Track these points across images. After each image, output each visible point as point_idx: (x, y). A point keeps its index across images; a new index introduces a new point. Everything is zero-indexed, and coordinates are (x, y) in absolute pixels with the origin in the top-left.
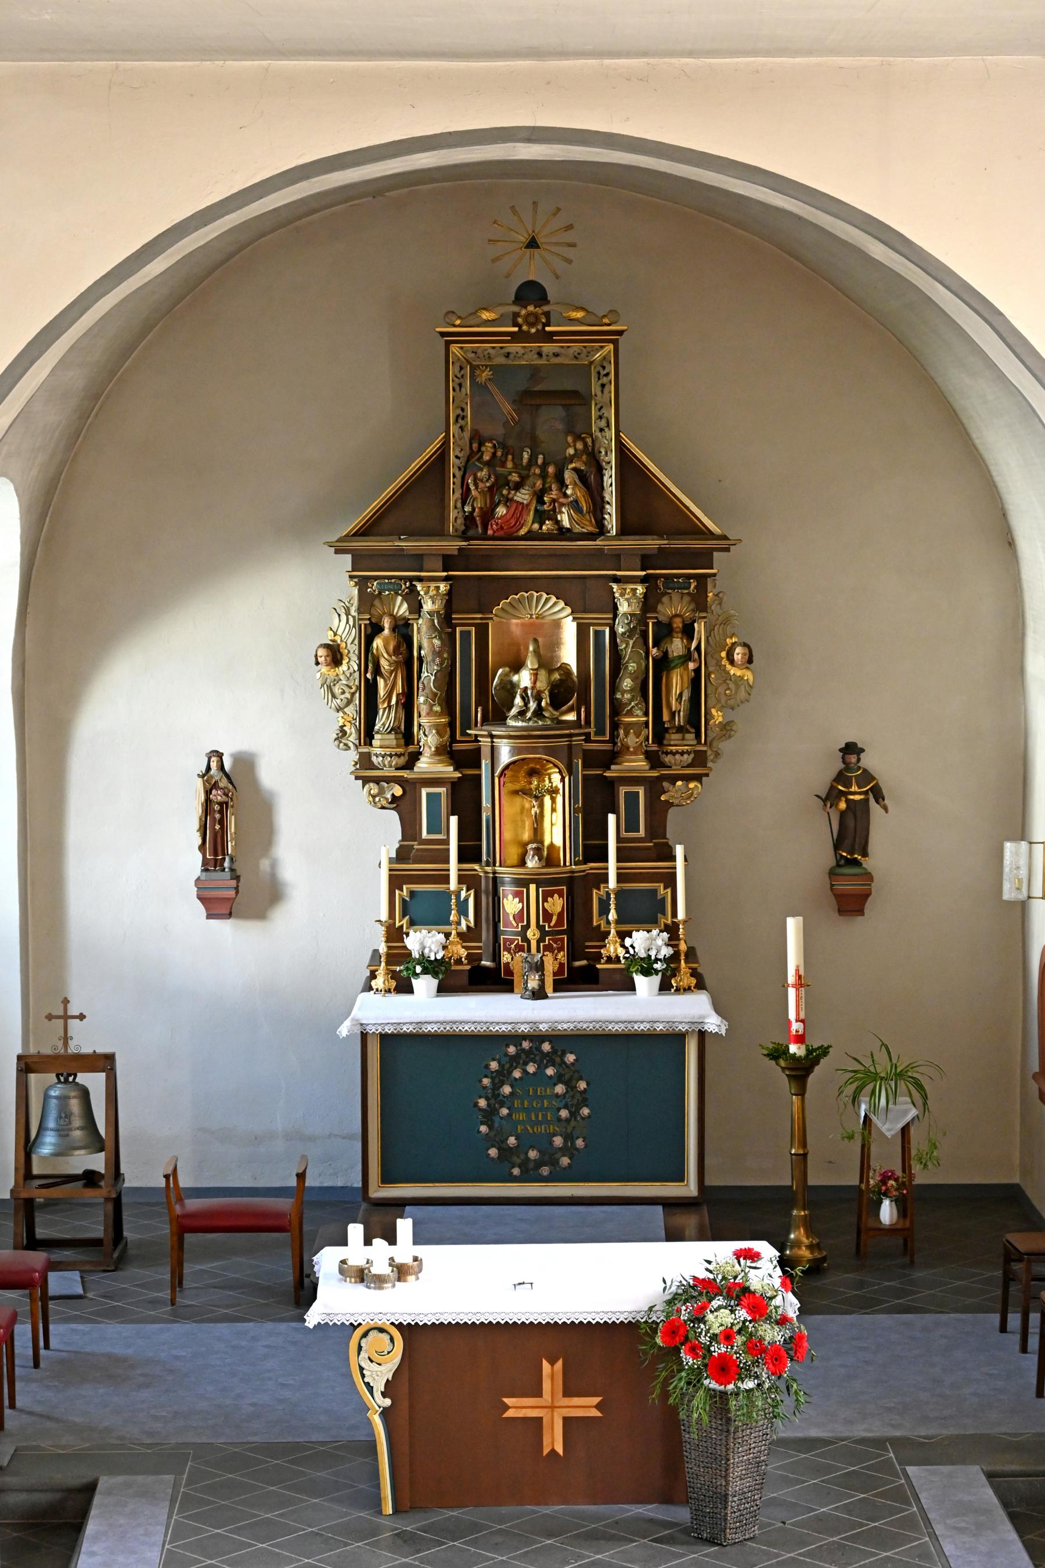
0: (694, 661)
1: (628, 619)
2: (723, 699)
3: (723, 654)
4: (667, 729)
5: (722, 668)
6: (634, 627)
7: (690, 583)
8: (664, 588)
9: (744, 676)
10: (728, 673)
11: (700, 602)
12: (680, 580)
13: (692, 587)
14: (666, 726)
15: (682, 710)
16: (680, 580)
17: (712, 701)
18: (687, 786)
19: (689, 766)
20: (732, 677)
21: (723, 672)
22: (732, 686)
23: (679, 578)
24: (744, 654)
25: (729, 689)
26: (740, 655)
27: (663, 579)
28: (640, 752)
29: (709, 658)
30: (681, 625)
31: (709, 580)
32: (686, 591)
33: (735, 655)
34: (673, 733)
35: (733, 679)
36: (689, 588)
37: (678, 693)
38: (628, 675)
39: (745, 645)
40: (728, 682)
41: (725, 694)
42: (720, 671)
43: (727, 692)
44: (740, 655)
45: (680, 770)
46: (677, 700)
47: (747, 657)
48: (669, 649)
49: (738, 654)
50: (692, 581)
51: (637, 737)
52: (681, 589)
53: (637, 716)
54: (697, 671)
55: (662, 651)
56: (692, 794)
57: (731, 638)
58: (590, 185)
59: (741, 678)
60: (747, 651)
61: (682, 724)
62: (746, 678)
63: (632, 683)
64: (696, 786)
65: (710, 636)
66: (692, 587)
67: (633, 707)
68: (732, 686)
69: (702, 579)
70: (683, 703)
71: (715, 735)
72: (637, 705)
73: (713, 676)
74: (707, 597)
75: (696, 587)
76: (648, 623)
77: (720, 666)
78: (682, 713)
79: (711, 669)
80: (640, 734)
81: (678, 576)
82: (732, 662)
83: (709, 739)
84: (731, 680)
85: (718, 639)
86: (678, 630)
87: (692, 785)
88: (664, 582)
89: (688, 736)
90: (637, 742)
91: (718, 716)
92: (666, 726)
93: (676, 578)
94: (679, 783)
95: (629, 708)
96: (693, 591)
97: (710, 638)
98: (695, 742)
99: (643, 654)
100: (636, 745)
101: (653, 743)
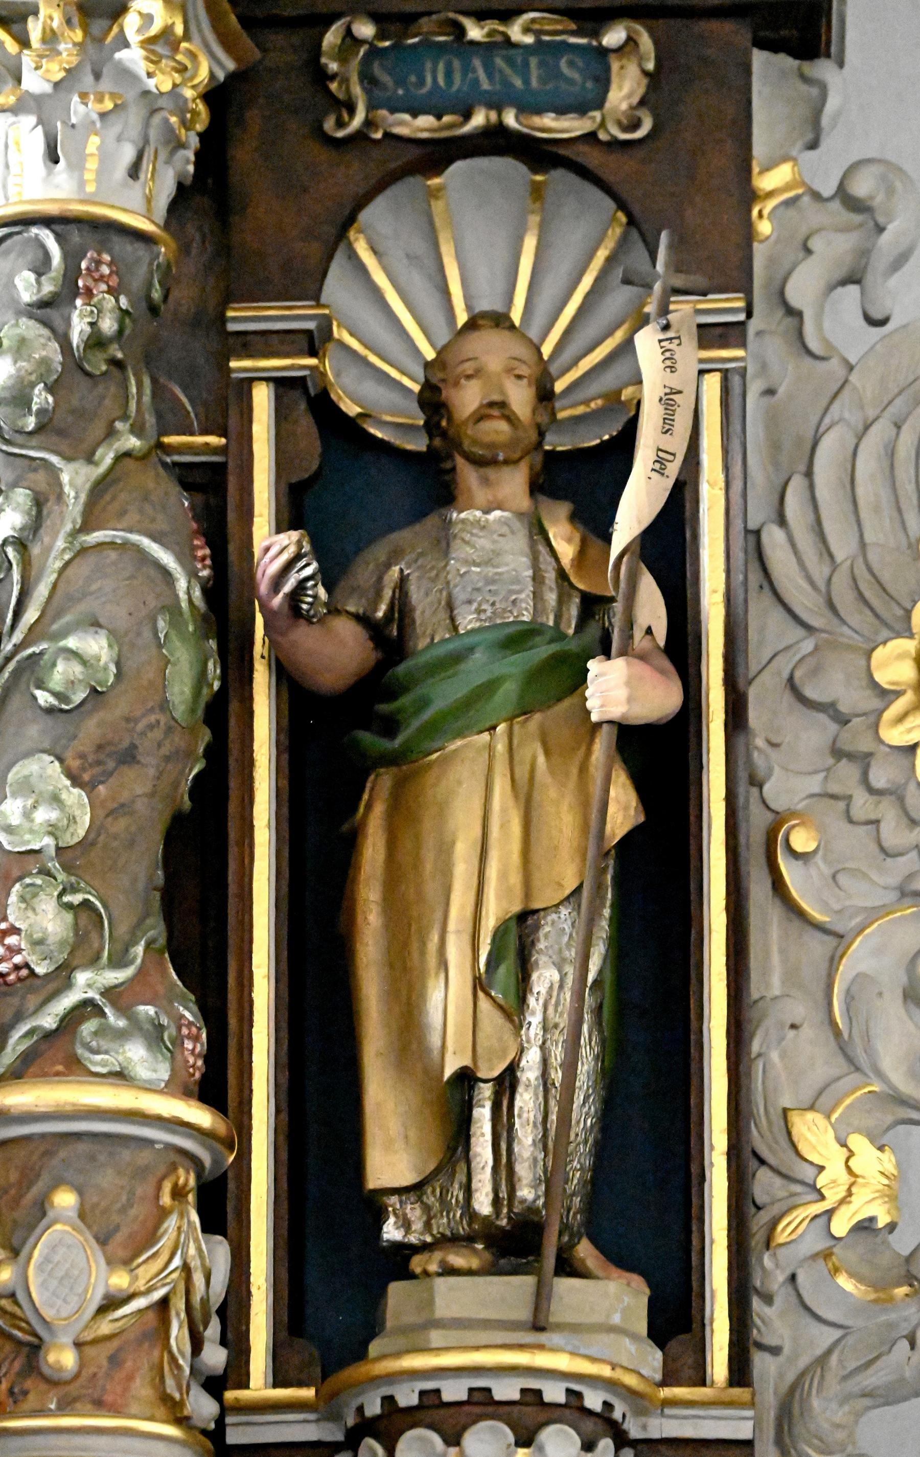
1: (41, 268)
4: (404, 1251)
5: (880, 777)
6: (96, 341)
8: (371, 107)
12: (516, 32)
14: (391, 1232)
15: (530, 1072)
16: (516, 32)
21: (888, 813)
23: (507, 16)
27: (365, 30)
28: (142, 1389)
34: (449, 1271)
36: (599, 104)
37: (490, 923)
38: (34, 731)
42: (862, 805)
46: (480, 985)
48: (416, 594)
50: (614, 37)
51: (127, 1262)
52: (526, 108)
53: (121, 1076)
55: (363, 620)
58: (233, 18)
61: (526, 1193)
63: (75, 797)
65: (782, 521)
67: (87, 1008)
70: (535, 1019)
71: (827, 1336)
72: (109, 992)
73: (802, 840)
74: (750, 196)
76: (246, 385)
77: (864, 760)
80: (152, 1237)
85: (843, 547)
86: (498, 429)
88: (374, 53)
90: (111, 1303)
92: (391, 1232)
93: (480, 16)
95: (48, 1020)
97: (774, 537)
99: (182, 584)
100: (105, 1327)
101: (279, 1380)
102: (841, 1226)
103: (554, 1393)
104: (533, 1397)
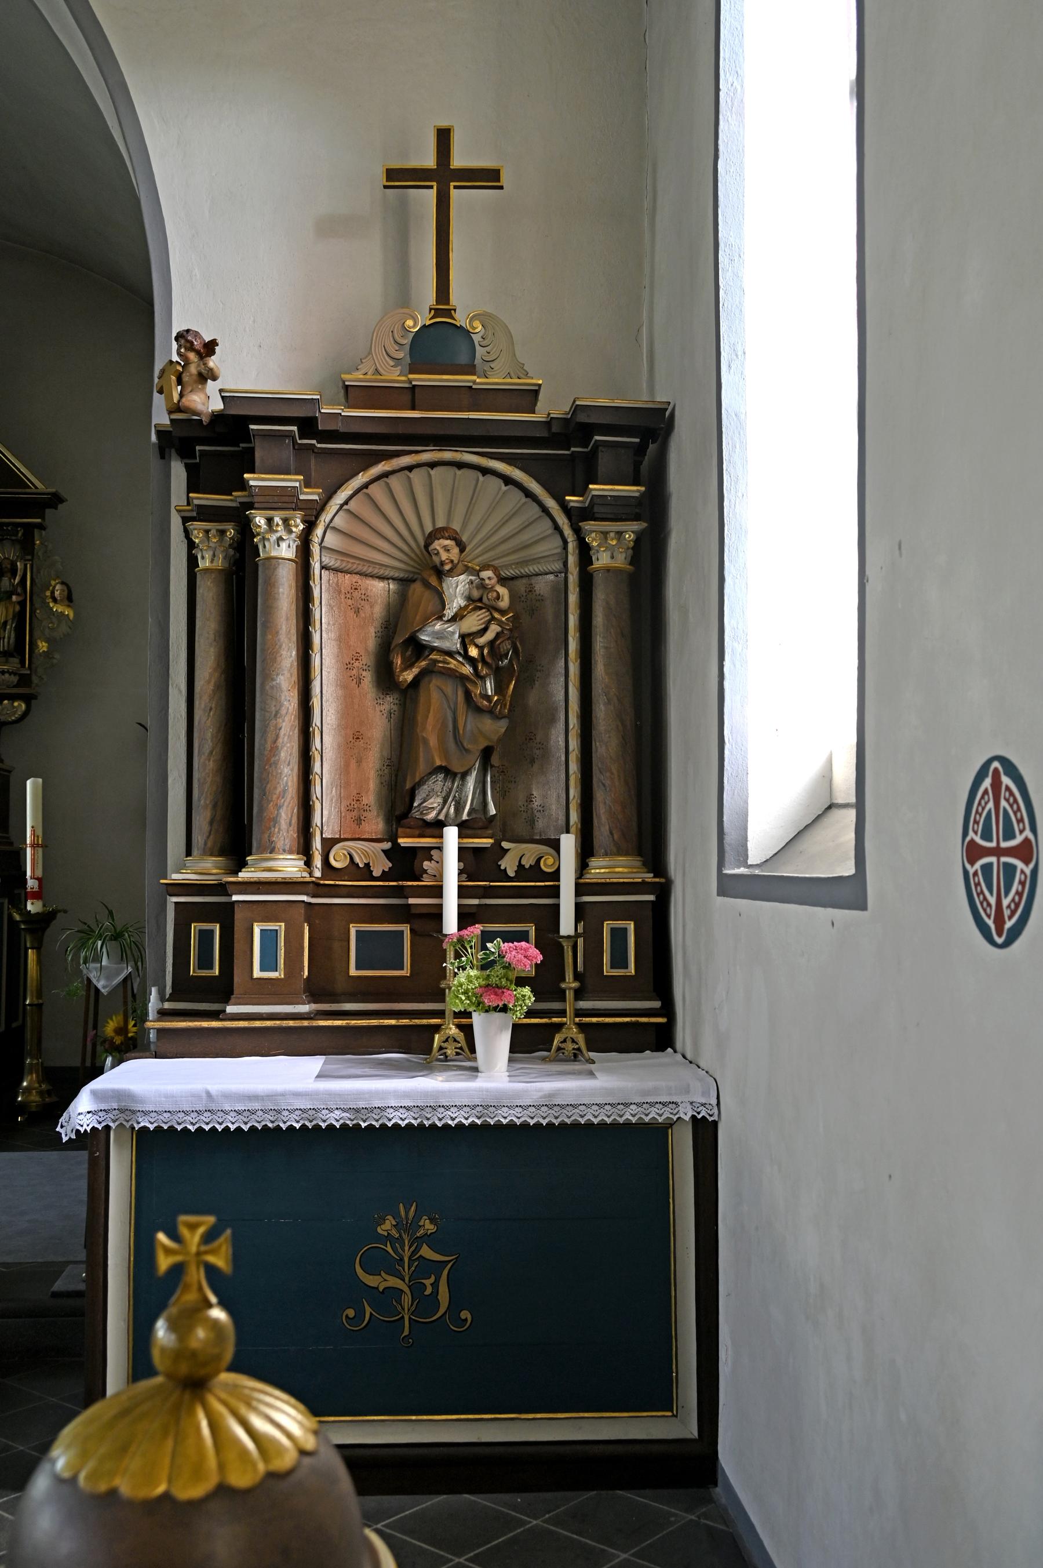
0: (18, 594)
2: (47, 631)
3: (48, 593)
7: (18, 532)
9: (65, 612)
10: (51, 609)
11: (27, 547)
12: (9, 528)
13: (20, 534)
16: (9, 528)
17: (37, 633)
18: (13, 704)
19: (15, 686)
20: (55, 613)
22: (54, 620)
23: (8, 526)
24: (62, 591)
25: (52, 623)
26: (59, 591)
29: (35, 597)
30: (9, 566)
31: (36, 531)
32: (14, 538)
33: (56, 592)
35: (56, 615)
36: (18, 534)
39: (63, 583)
40: (52, 617)
41: (49, 627)
43: (50, 625)
44: (59, 591)
45: (5, 689)
47: (66, 593)
49: (57, 591)
54: (22, 604)
56: (15, 712)
57: (55, 580)
59: (62, 613)
60: (65, 588)
62: (67, 613)
64: (19, 704)
66: (20, 534)
68: (54, 620)
69: (29, 528)
73: (38, 611)
74: (35, 544)
75: (23, 534)
78: (6, 640)
79: (37, 605)
81: (8, 524)
82: (55, 600)
83: (34, 666)
84: (54, 615)
87: (16, 704)
89: (11, 659)
91: (43, 646)
94: (6, 702)
96: (21, 538)
98: (19, 666)
102: (41, 651)
103: (6, 670)
104: (3, 671)
